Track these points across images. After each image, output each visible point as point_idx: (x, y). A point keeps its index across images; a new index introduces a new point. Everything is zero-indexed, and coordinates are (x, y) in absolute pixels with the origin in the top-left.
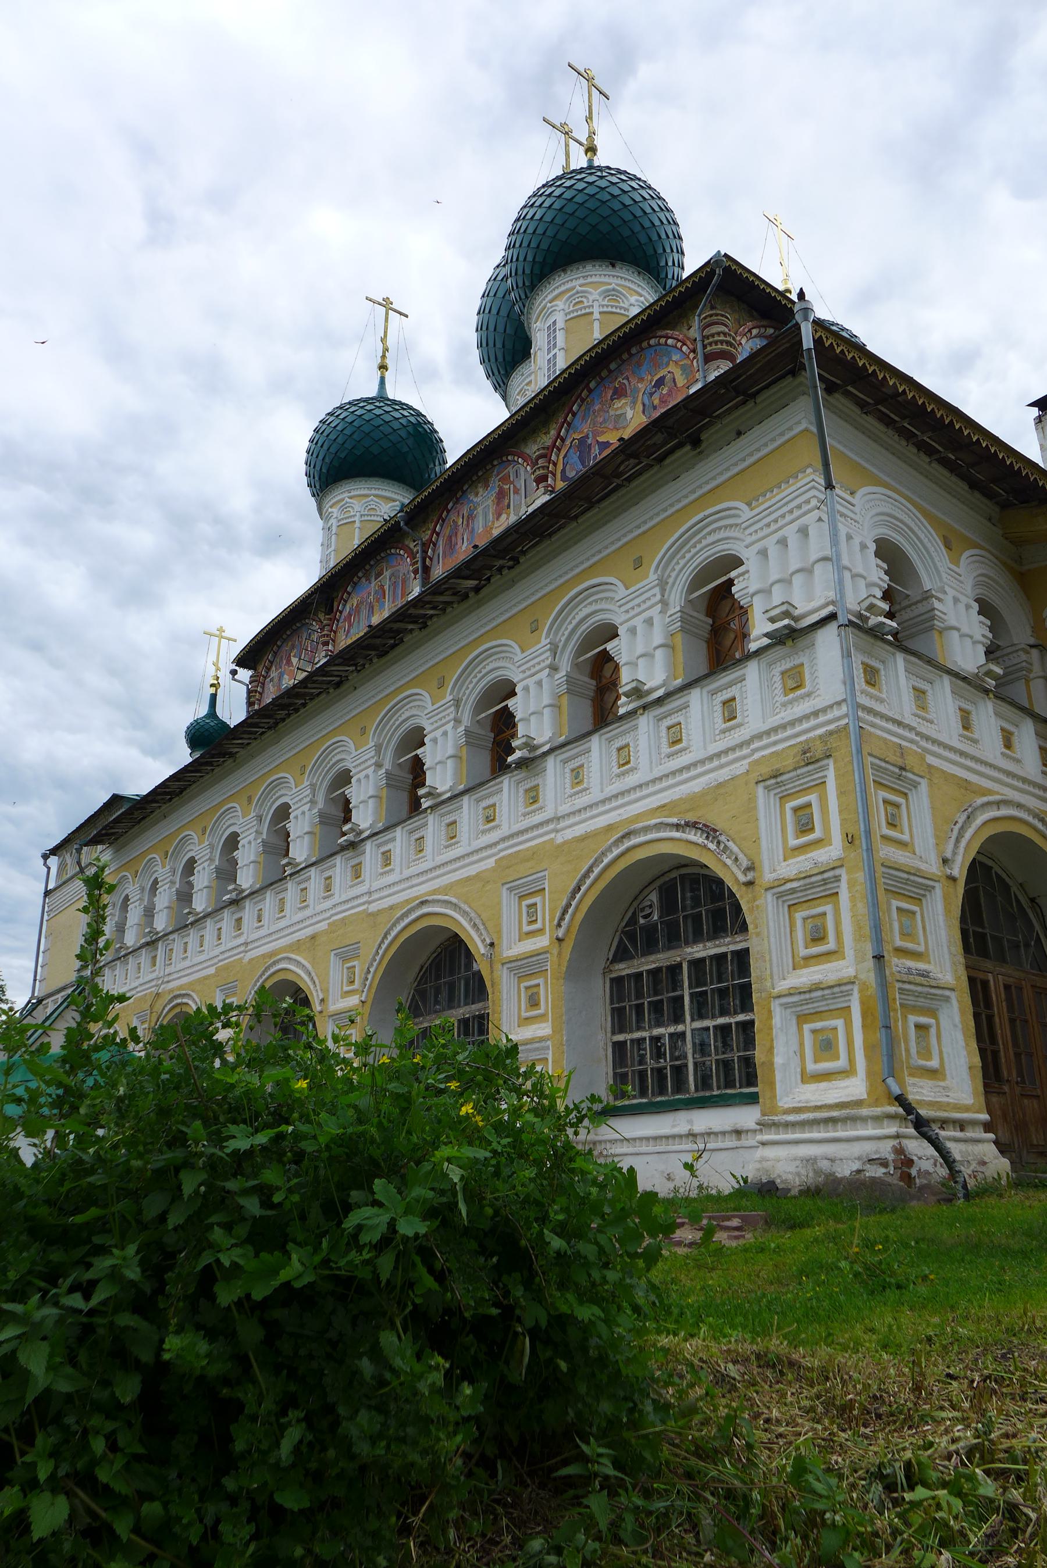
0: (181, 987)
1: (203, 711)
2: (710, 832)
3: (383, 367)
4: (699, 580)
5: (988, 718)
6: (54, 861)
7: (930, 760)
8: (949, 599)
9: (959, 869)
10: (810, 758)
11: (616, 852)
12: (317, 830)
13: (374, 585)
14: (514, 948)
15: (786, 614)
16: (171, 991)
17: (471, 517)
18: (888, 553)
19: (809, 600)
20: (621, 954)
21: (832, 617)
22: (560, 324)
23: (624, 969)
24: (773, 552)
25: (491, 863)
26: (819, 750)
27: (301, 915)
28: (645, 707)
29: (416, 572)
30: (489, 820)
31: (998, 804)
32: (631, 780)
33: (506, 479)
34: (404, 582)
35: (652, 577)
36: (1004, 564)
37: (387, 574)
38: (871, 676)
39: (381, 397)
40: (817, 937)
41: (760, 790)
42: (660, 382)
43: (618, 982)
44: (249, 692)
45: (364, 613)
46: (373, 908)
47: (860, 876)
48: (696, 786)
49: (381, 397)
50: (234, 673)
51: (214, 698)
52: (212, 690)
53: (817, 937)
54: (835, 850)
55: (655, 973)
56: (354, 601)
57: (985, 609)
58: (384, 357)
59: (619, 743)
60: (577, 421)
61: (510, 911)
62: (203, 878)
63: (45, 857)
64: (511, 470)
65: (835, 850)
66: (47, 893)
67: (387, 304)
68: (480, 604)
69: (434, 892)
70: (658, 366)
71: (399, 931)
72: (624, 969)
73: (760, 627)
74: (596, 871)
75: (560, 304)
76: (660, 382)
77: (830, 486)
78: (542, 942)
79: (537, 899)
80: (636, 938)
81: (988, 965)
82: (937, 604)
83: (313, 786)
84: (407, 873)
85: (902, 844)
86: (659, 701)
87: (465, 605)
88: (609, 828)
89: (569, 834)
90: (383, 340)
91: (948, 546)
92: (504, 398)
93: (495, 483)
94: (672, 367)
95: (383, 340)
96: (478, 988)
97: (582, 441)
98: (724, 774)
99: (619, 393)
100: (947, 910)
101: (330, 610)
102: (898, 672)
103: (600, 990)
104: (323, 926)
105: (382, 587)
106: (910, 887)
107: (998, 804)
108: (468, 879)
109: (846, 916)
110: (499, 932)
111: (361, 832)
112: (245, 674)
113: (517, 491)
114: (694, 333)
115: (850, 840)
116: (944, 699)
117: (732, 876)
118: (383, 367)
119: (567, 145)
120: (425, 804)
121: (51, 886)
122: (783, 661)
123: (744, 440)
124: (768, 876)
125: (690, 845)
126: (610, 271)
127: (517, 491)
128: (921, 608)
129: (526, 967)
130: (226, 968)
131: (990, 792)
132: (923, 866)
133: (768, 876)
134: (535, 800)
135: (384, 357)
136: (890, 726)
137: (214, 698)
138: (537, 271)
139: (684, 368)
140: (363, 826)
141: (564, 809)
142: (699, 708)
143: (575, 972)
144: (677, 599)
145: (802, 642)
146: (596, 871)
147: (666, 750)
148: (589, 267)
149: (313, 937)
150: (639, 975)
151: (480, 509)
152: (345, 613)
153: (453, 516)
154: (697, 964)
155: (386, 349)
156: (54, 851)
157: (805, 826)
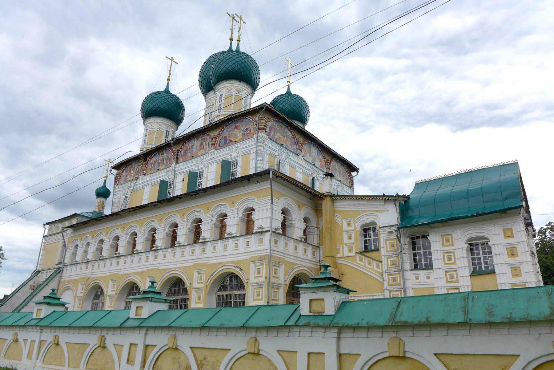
0: (97, 277)
1: (102, 185)
2: (241, 269)
3: (169, 80)
4: (246, 210)
5: (301, 247)
6: (47, 226)
7: (286, 259)
8: (297, 220)
9: (288, 282)
10: (261, 259)
11: (221, 269)
12: (145, 242)
13: (160, 157)
14: (196, 285)
15: (261, 228)
16: (93, 278)
17: (192, 147)
18: (284, 212)
19: (266, 225)
20: (220, 290)
21: (269, 231)
22: (223, 96)
23: (220, 293)
24: (261, 211)
25: (192, 264)
26: (263, 258)
27: (138, 265)
28: (231, 237)
29: (174, 158)
30: (193, 253)
31: (299, 267)
32: (226, 253)
33: (203, 140)
34: (170, 159)
35: (236, 207)
36: (312, 208)
37: (165, 155)
38: (276, 242)
39: (167, 90)
40: (258, 295)
41: (251, 263)
42: (247, 129)
43: (218, 296)
44: (116, 178)
45: (157, 165)
46: (160, 268)
47: (267, 285)
48: (239, 259)
49: (167, 90)
50: (111, 171)
51: (105, 181)
52: (105, 178)
53: (258, 295)
54: (263, 279)
55: (227, 295)
56: (153, 160)
57: (306, 220)
58: (169, 76)
59: (224, 244)
60: (225, 131)
61: (196, 276)
62: (106, 247)
63: (44, 225)
64: (205, 138)
65: (263, 279)
66: (44, 237)
67: (172, 59)
68: (195, 198)
69: (177, 268)
70: (247, 124)
71: (167, 276)
72: (220, 293)
73: (256, 229)
74: (217, 272)
75: (224, 90)
76: (247, 129)
77: (272, 203)
78: (203, 285)
79: (202, 275)
80: (223, 287)
81: (294, 299)
82: (294, 222)
83: (144, 230)
84: (170, 261)
85: (277, 277)
86: (234, 237)
87: (192, 197)
88: (220, 263)
89: (211, 262)
90: (170, 71)
91: (299, 207)
92: (205, 97)
93: (200, 139)
94: (250, 126)
95: (170, 71)
96: (186, 291)
97: (225, 137)
98: (245, 258)
99: (236, 128)
100: (284, 291)
101: (145, 160)
102: (282, 240)
103: (214, 297)
104: (145, 269)
105: (163, 158)
106: (277, 287)
107: (299, 267)
108: (186, 267)
109: (263, 292)
110: (193, 281)
111: (158, 247)
112: (115, 171)
113: (206, 145)
114: (257, 119)
115: (266, 278)
116: (291, 244)
117: (244, 280)
118: (169, 80)
119: (233, 22)
120: (176, 245)
121: (46, 234)
122: (259, 237)
123: (258, 184)
124: (251, 282)
125: (237, 271)
126: (239, 83)
127: (206, 145)
128: (291, 222)
129: (198, 290)
130: (113, 275)
131: (298, 264)
132: (280, 282)
133: (251, 282)
134: (204, 251)
135: (169, 76)
136: (278, 253)
137: (105, 181)
138: (219, 78)
139: (253, 128)
140: (159, 245)
141: (210, 255)
142: (242, 241)
143: (209, 293)
144: (240, 215)
145: (263, 234)
146: (217, 272)
147: (234, 248)
148: (233, 81)
149: (142, 272)
150: (223, 295)
151: (195, 146)
152: (151, 162)
153: (187, 145)
154: (235, 295)
155: (170, 74)
156: (47, 224)
157: (259, 273)
